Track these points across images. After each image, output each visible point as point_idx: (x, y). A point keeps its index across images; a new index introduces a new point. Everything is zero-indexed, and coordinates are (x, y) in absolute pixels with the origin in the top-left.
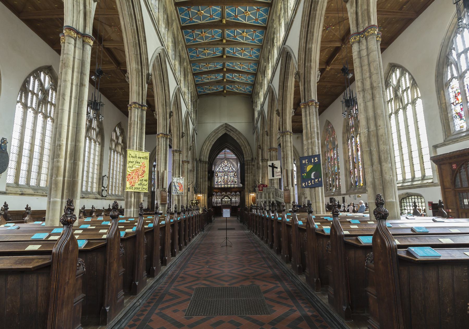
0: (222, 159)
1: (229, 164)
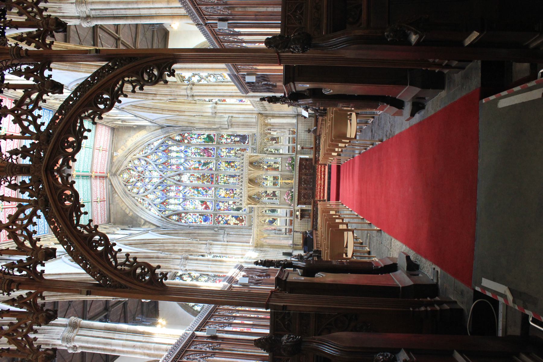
0: (112, 191)
1: (136, 162)
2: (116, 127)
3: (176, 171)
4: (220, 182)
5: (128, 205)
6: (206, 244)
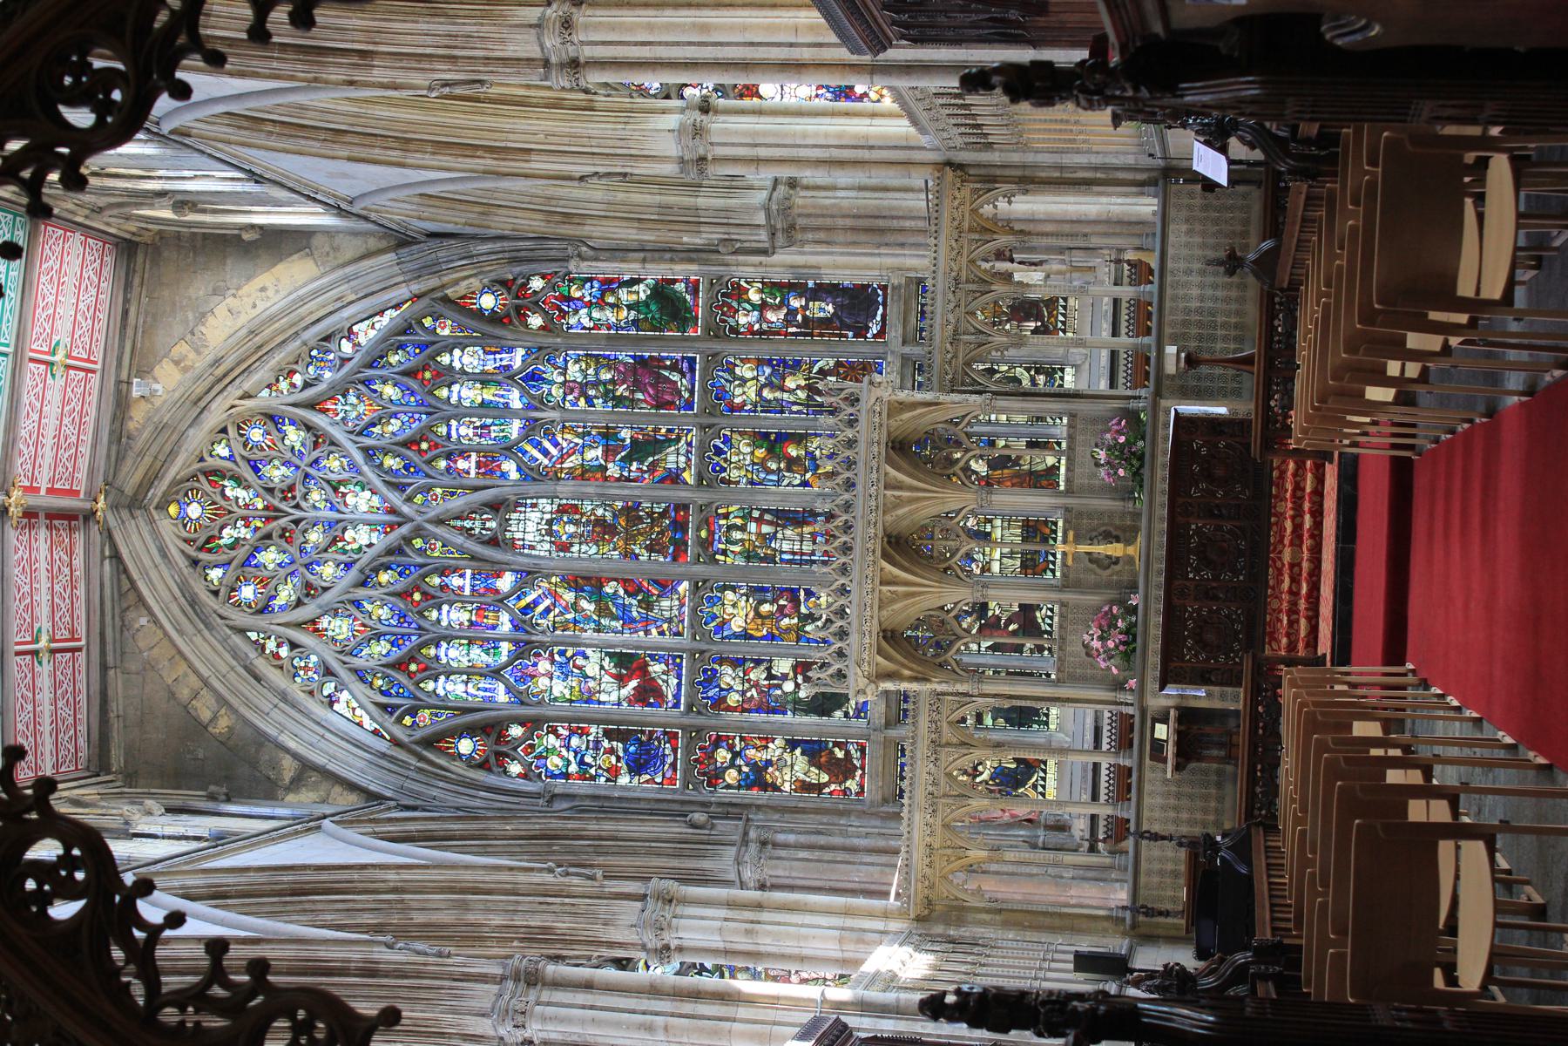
2: (147, 238)
3: (476, 489)
4: (724, 552)
5: (205, 672)
6: (643, 898)
